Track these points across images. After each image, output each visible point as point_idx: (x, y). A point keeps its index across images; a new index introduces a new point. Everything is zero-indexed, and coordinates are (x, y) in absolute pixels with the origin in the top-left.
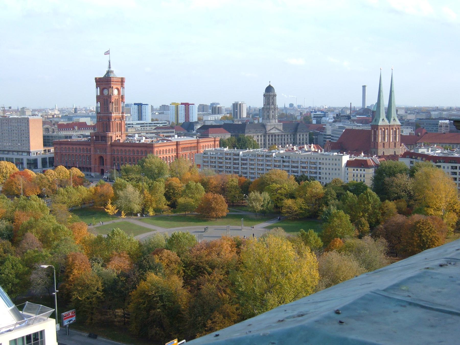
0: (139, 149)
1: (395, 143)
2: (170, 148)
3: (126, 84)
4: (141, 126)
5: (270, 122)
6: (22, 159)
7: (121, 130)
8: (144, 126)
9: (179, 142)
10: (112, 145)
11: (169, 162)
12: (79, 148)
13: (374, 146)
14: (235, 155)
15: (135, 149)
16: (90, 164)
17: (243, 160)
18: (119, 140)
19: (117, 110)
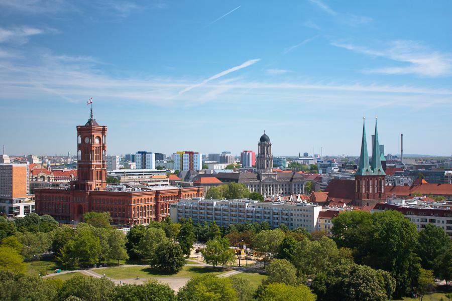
0: (117, 198)
1: (380, 195)
2: (150, 197)
3: (107, 133)
4: (139, 175)
5: (264, 172)
6: (4, 207)
7: (101, 179)
8: (142, 175)
9: (159, 191)
10: (91, 193)
11: (138, 212)
12: (60, 196)
13: (358, 197)
14: (209, 205)
15: (114, 198)
16: (70, 213)
17: (216, 210)
18: (99, 188)
19: (98, 158)
